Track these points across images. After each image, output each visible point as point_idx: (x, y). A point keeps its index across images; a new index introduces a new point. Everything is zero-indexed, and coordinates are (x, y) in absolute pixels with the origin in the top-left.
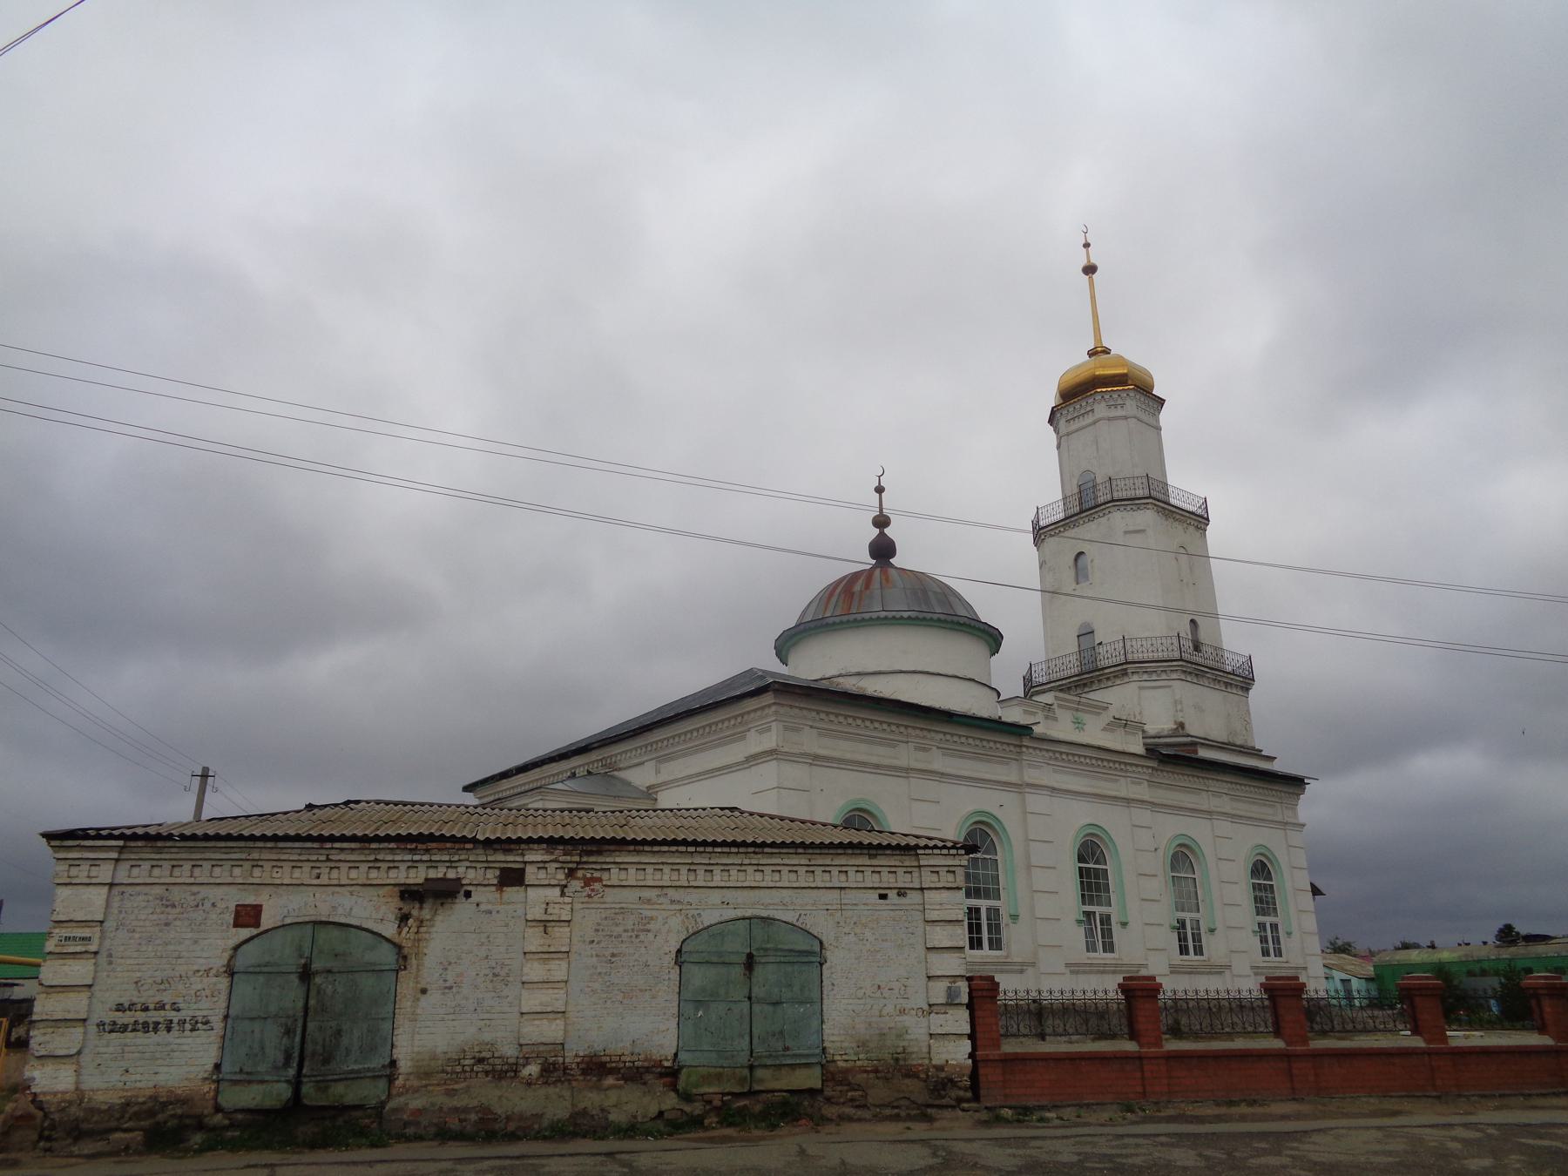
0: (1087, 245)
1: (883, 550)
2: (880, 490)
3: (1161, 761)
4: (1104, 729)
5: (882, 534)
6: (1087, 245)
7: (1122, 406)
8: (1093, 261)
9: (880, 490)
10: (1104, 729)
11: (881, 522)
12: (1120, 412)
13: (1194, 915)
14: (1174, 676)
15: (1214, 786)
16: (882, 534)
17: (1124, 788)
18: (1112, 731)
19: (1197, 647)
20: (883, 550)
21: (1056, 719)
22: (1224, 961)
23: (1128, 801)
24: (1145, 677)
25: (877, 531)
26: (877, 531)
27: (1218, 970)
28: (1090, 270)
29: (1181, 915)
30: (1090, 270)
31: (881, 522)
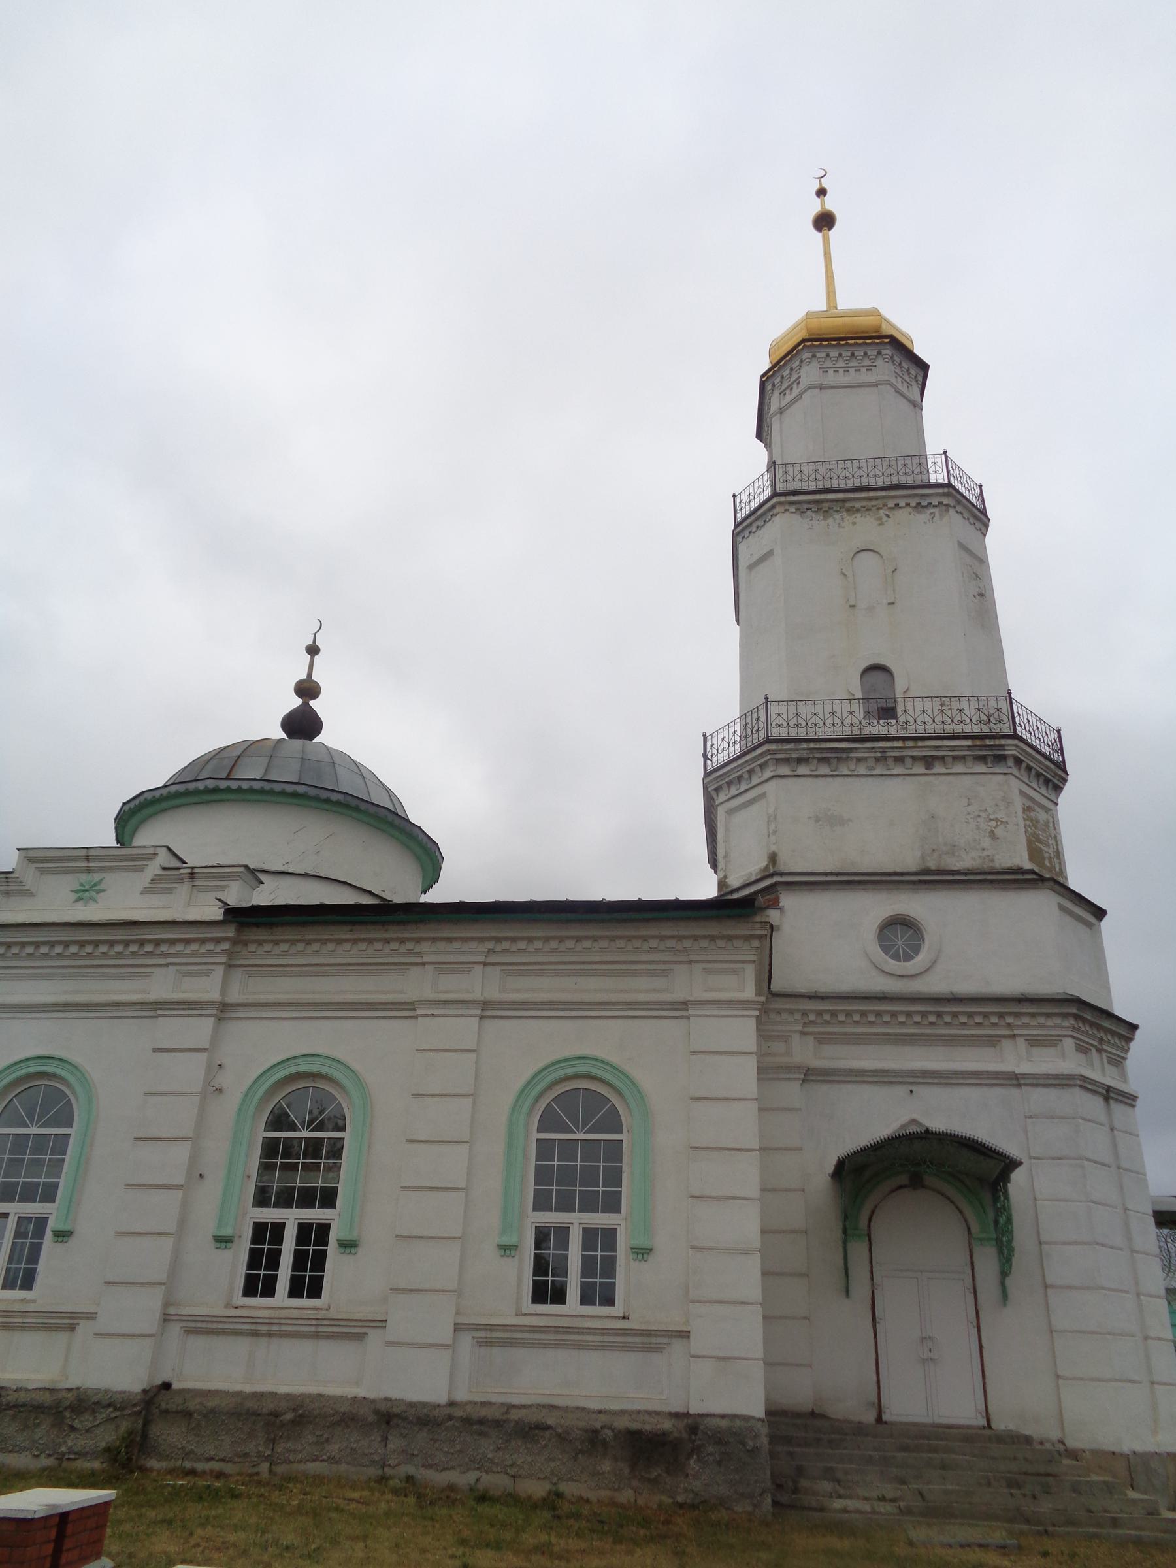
0: (822, 192)
1: (302, 724)
2: (313, 650)
3: (242, 926)
4: (145, 892)
5: (306, 705)
6: (822, 192)
7: (797, 381)
8: (829, 206)
9: (313, 650)
10: (145, 892)
11: (307, 689)
12: (796, 392)
13: (315, 1215)
14: (768, 774)
15: (431, 952)
16: (306, 705)
17: (161, 984)
18: (170, 891)
19: (888, 713)
20: (302, 724)
21: (29, 894)
22: (674, 1321)
23: (154, 1007)
24: (734, 791)
25: (298, 702)
26: (298, 702)
27: (353, 1331)
28: (825, 221)
29: (271, 1214)
30: (825, 221)
31: (307, 689)
